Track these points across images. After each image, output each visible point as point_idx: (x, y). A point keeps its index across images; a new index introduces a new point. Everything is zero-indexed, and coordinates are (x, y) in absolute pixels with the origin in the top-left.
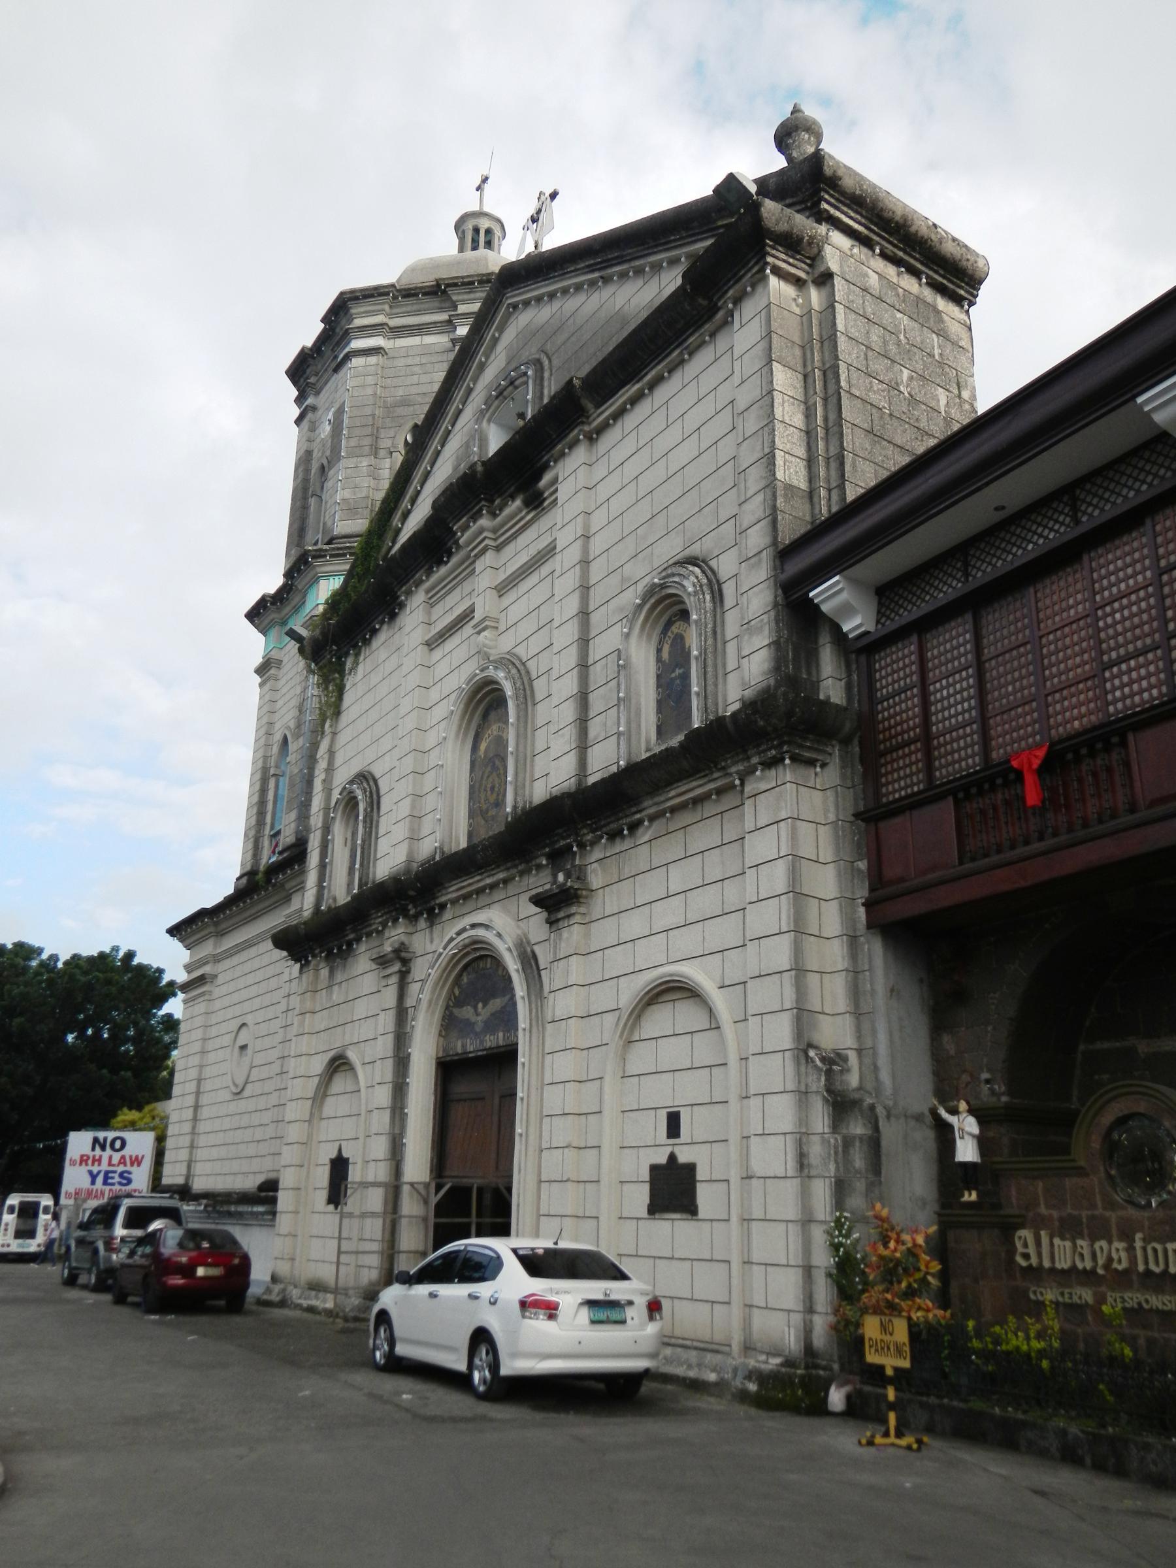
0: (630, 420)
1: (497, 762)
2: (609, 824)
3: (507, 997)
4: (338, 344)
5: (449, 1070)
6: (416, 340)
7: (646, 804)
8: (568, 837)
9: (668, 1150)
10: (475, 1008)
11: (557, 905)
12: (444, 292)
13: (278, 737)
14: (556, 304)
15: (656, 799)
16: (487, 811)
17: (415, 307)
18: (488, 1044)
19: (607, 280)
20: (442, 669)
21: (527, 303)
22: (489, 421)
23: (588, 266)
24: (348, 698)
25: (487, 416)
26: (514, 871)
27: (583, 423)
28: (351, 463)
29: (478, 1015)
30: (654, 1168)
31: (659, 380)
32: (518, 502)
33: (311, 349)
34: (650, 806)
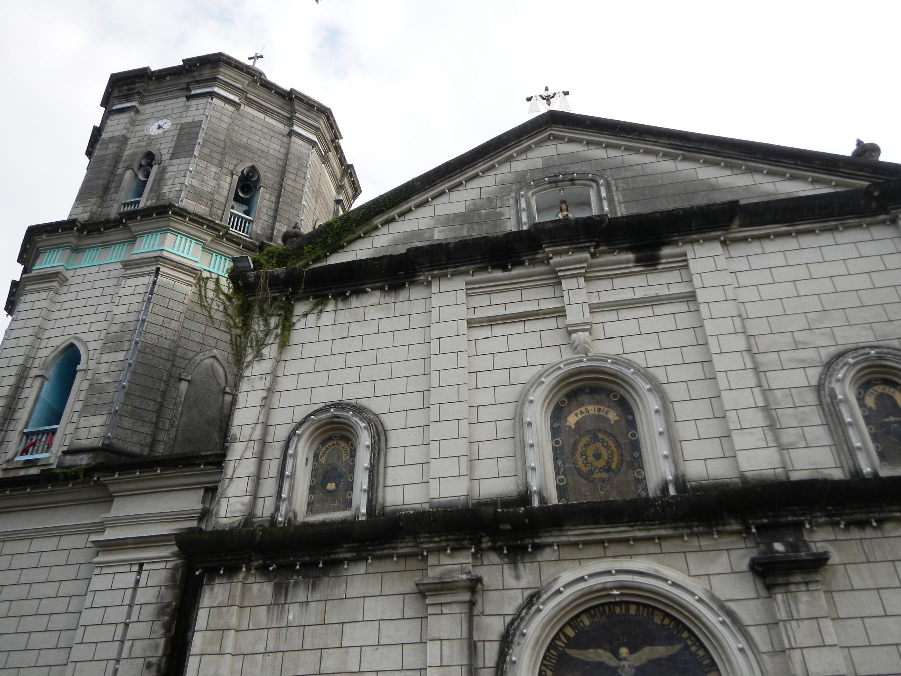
0: (770, 246)
1: (600, 436)
2: (854, 513)
4: (198, 82)
6: (262, 116)
8: (804, 515)
10: (615, 654)
12: (291, 99)
13: (54, 341)
14: (612, 153)
17: (266, 96)
19: (685, 159)
20: (483, 346)
21: (571, 140)
22: (533, 194)
24: (296, 336)
25: (533, 191)
27: (726, 230)
28: (203, 164)
29: (620, 660)
32: (631, 256)
33: (153, 72)
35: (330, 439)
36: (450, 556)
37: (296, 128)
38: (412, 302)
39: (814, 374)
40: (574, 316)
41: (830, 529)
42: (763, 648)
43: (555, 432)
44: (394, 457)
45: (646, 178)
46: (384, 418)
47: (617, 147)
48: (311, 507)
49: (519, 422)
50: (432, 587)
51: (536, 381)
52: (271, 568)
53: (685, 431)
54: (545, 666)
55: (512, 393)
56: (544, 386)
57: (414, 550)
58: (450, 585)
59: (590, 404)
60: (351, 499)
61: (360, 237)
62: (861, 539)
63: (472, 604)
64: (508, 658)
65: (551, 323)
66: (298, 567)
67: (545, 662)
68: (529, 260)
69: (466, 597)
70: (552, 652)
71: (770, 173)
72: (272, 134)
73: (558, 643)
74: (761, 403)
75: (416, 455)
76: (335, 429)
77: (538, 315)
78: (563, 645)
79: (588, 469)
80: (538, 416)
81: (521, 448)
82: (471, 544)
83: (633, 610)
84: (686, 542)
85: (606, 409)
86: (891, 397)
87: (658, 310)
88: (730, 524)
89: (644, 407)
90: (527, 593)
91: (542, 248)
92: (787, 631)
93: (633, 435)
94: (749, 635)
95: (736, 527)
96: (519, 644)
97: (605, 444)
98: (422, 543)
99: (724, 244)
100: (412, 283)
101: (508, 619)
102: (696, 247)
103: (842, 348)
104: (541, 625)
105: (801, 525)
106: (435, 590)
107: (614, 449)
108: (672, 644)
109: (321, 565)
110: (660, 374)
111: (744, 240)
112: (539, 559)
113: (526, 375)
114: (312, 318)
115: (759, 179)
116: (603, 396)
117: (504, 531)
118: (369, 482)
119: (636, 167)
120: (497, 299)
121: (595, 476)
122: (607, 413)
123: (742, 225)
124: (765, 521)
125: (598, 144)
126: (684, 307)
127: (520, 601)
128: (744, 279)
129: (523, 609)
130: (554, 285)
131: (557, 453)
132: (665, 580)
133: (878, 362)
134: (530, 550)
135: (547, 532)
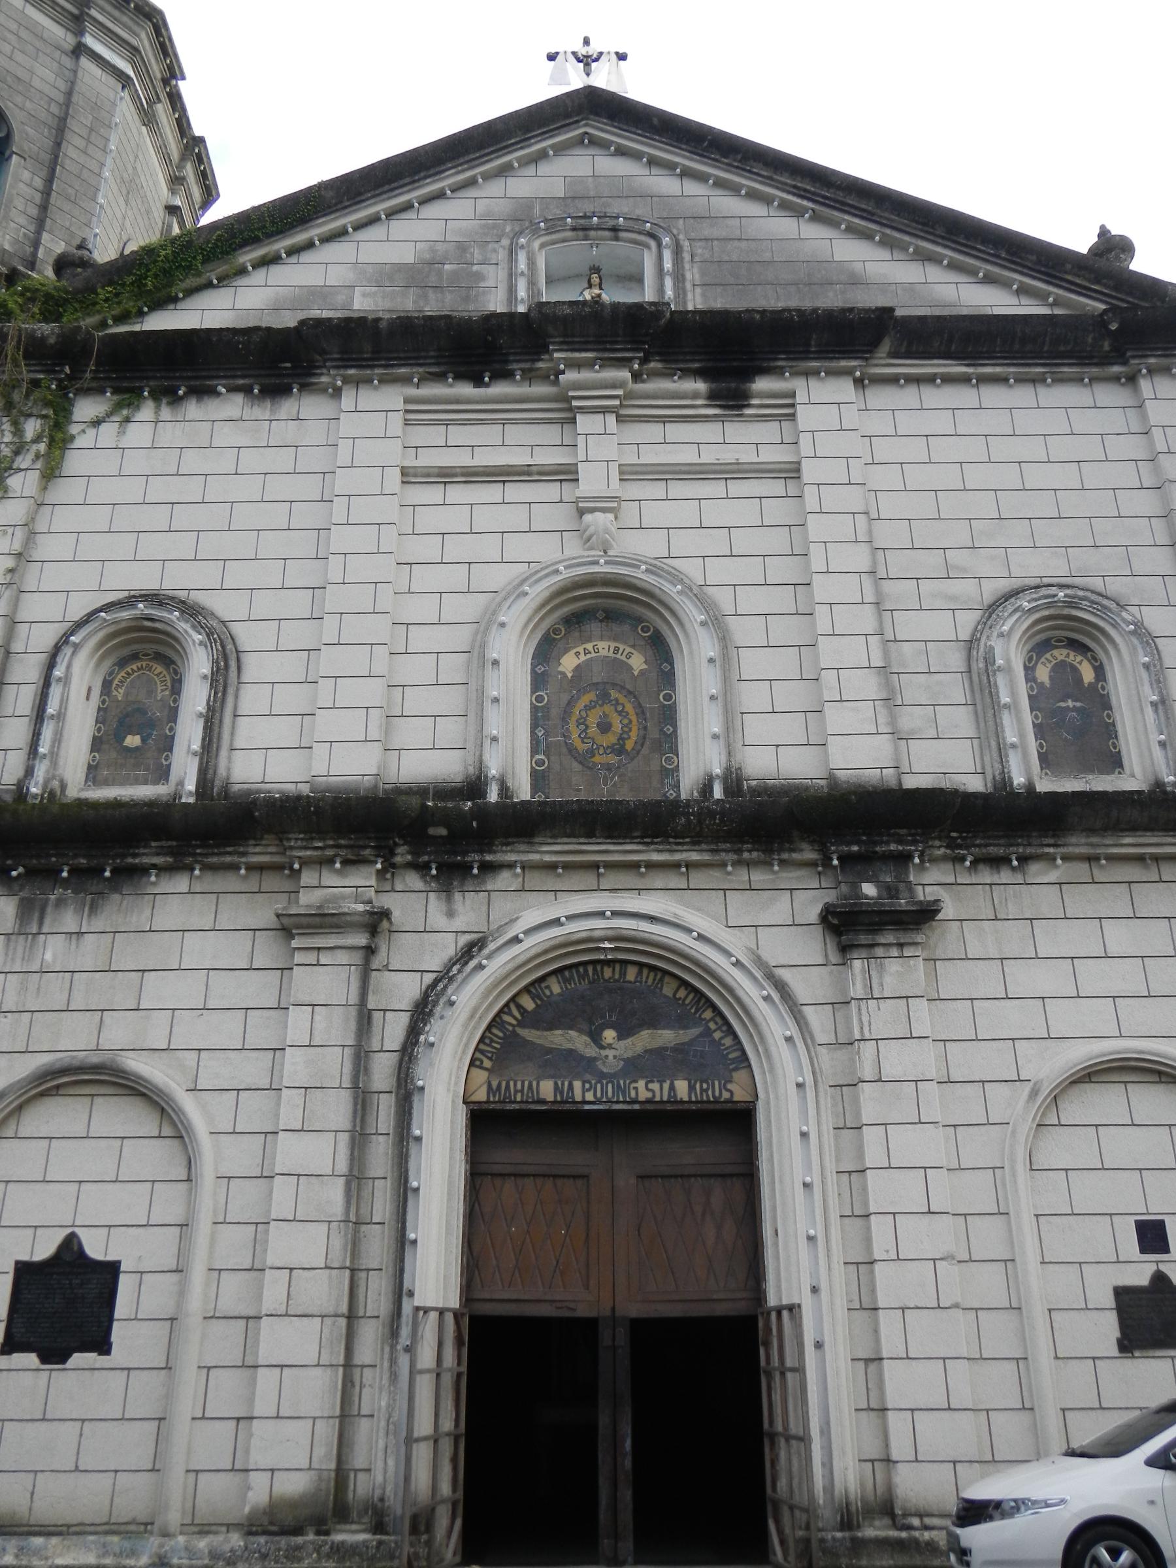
0: (933, 396)
1: (614, 694)
2: (986, 846)
3: (694, 1032)
5: (486, 1124)
7: (1074, 840)
8: (915, 842)
9: (1152, 1268)
11: (848, 928)
14: (692, 188)
15: (1094, 840)
16: (592, 753)
18: (644, 1095)
19: (816, 218)
20: (429, 520)
21: (621, 152)
22: (542, 246)
23: (795, 187)
24: (75, 462)
26: (732, 857)
27: (867, 359)
29: (602, 1047)
30: (1123, 1294)
31: (1002, 380)
32: (701, 386)
34: (1078, 844)
35: (135, 657)
36: (338, 872)
37: (89, 40)
38: (303, 419)
39: (968, 621)
40: (592, 482)
41: (949, 866)
42: (821, 1038)
43: (538, 681)
44: (251, 699)
45: (743, 244)
46: (237, 629)
47: (701, 178)
48: (93, 774)
49: (478, 658)
50: (304, 920)
51: (516, 591)
52: (14, 873)
53: (752, 697)
54: (482, 1052)
55: (472, 607)
56: (527, 600)
57: (277, 859)
58: (335, 920)
59: (602, 639)
60: (169, 766)
61: (209, 285)
62: (991, 885)
63: (370, 951)
64: (422, 1038)
65: (551, 491)
66: (65, 874)
67: (482, 1047)
68: (523, 370)
69: (361, 940)
70: (495, 1031)
71: (953, 266)
72: (39, 44)
73: (507, 1018)
74: (877, 662)
75: (291, 699)
76: (144, 640)
77: (529, 474)
78: (514, 1022)
79: (586, 747)
80: (512, 651)
81: (478, 703)
82: (378, 856)
83: (631, 973)
84: (729, 874)
85: (628, 650)
86: (1075, 670)
87: (736, 488)
88: (802, 850)
89: (691, 653)
90: (464, 939)
91: (547, 351)
92: (860, 1014)
93: (668, 697)
94: (804, 1018)
95: (809, 854)
96: (442, 1017)
97: (620, 708)
98: (291, 848)
99: (859, 383)
100: (304, 387)
101: (429, 978)
102: (813, 382)
103: (1016, 584)
104: (482, 989)
105: (906, 858)
106: (309, 926)
107: (634, 718)
108: (685, 1027)
109: (107, 874)
110: (724, 599)
111: (893, 380)
112: (489, 888)
113: (499, 578)
114: (109, 430)
115: (934, 273)
116: (626, 628)
117: (435, 837)
118: (204, 739)
119: (730, 222)
120: (458, 435)
121: (597, 759)
122: (629, 656)
123: (894, 354)
124: (855, 848)
125: (670, 167)
126: (777, 487)
127: (451, 951)
128: (884, 450)
129: (454, 964)
130: (562, 422)
131: (538, 717)
132: (689, 931)
133: (1066, 611)
134: (475, 871)
135: (507, 844)
